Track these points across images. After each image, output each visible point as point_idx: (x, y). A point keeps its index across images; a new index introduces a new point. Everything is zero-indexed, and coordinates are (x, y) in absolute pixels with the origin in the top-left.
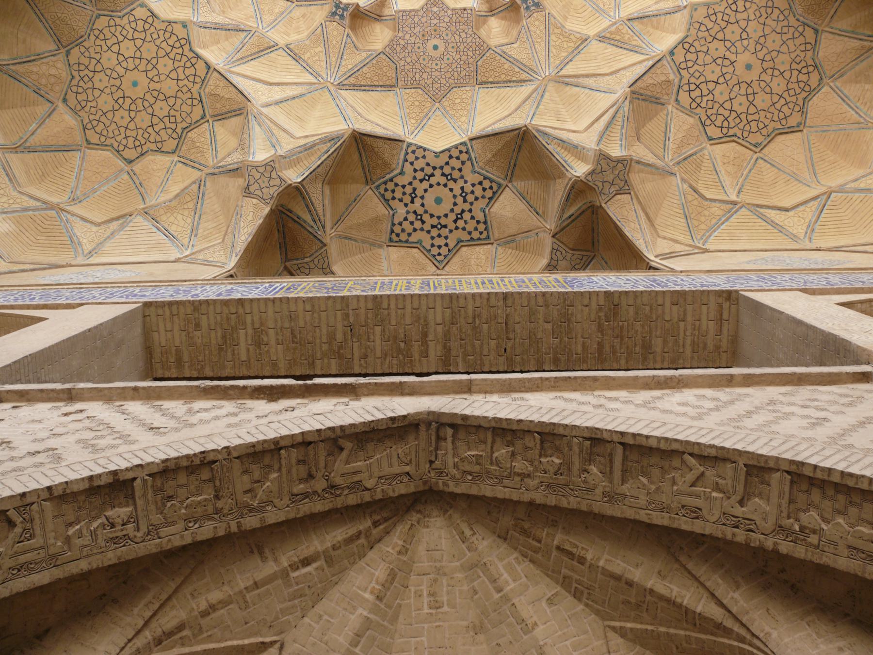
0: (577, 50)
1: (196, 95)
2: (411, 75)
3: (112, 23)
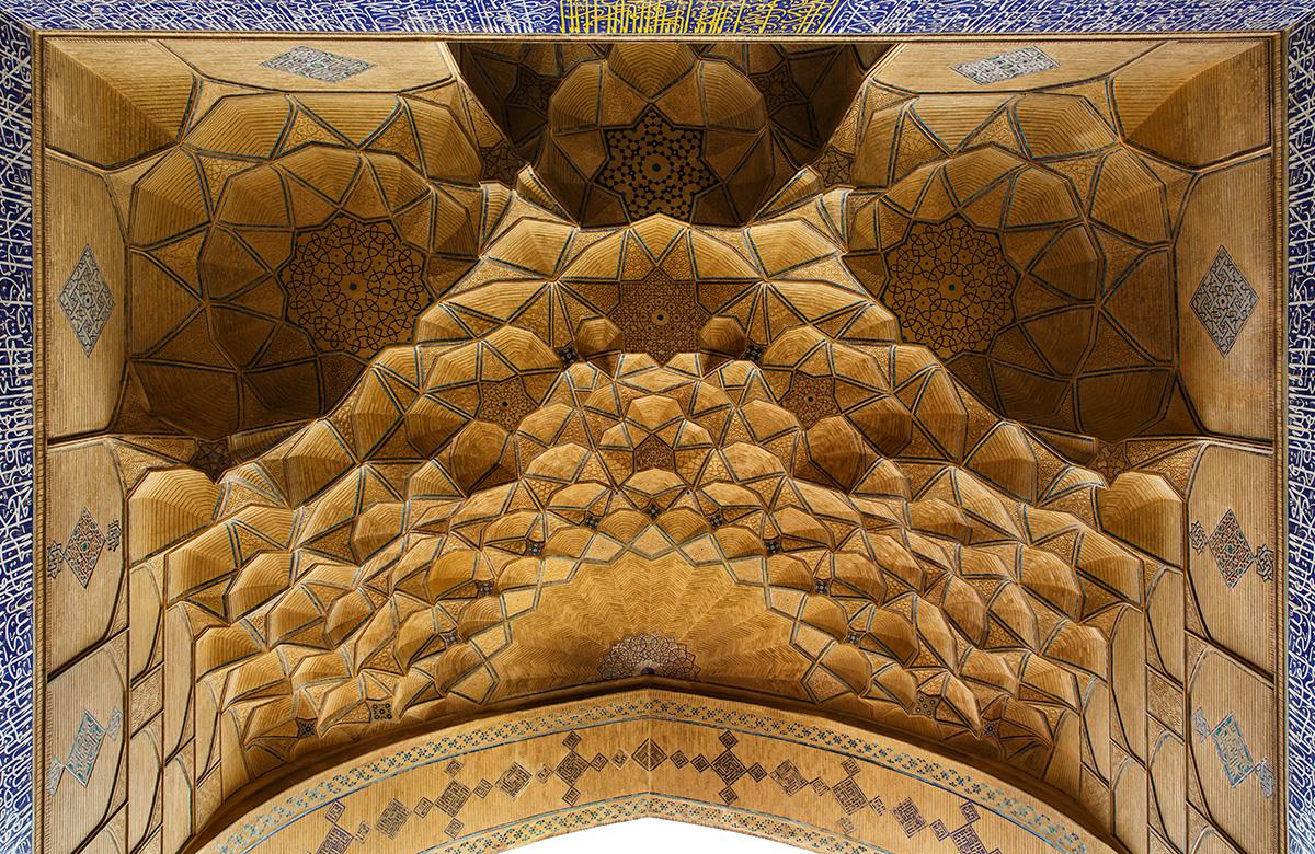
0: (523, 310)
1: (894, 275)
2: (684, 293)
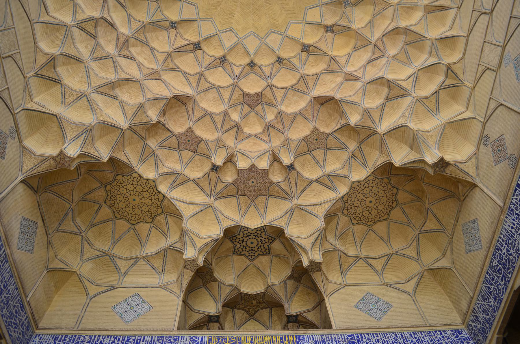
0: (307, 186)
3: (123, 178)
